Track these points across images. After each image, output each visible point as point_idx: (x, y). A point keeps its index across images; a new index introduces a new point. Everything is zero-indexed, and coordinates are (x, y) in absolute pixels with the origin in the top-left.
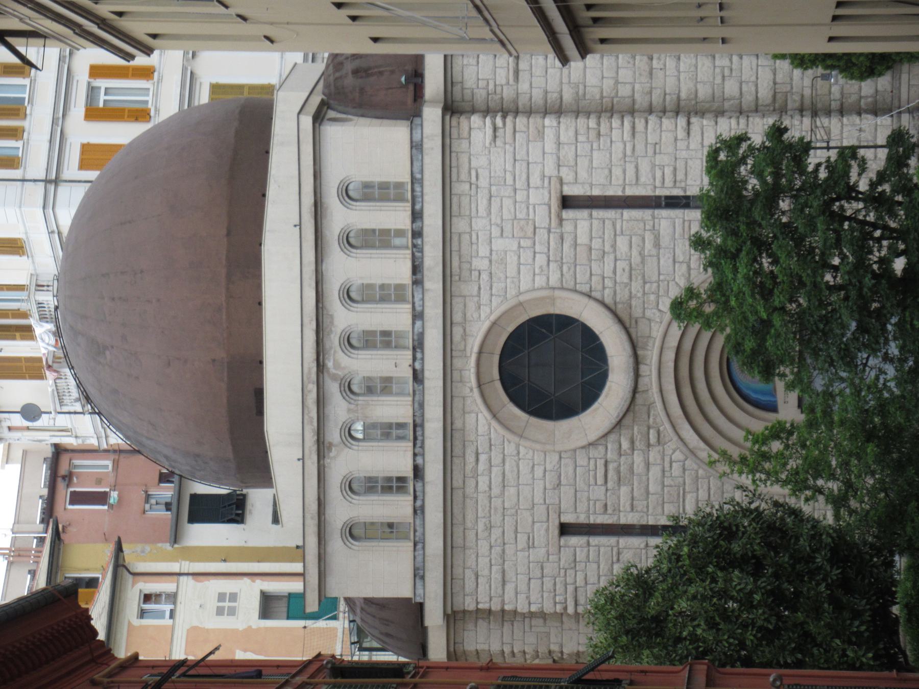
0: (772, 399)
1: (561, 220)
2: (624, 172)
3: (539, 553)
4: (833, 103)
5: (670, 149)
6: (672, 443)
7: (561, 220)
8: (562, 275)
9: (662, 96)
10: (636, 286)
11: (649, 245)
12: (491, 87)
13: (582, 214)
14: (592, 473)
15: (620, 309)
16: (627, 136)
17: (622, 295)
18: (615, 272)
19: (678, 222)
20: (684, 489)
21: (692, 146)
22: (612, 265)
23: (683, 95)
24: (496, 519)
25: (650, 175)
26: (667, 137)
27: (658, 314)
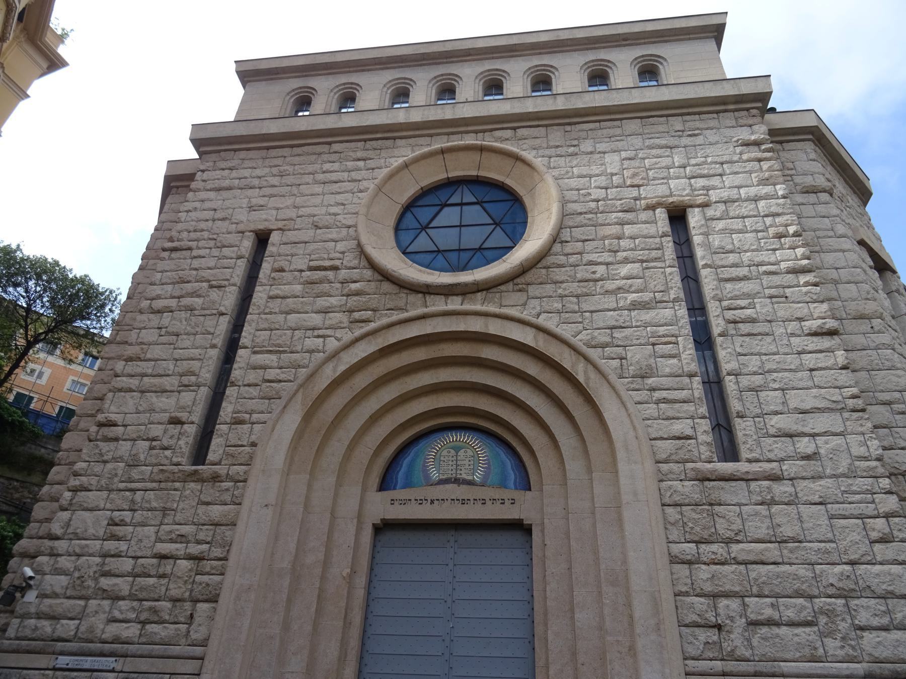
1: (652, 208)
3: (242, 216)
7: (652, 208)
8: (581, 213)
10: (574, 287)
18: (591, 263)
19: (673, 329)
20: (284, 352)
24: (290, 180)
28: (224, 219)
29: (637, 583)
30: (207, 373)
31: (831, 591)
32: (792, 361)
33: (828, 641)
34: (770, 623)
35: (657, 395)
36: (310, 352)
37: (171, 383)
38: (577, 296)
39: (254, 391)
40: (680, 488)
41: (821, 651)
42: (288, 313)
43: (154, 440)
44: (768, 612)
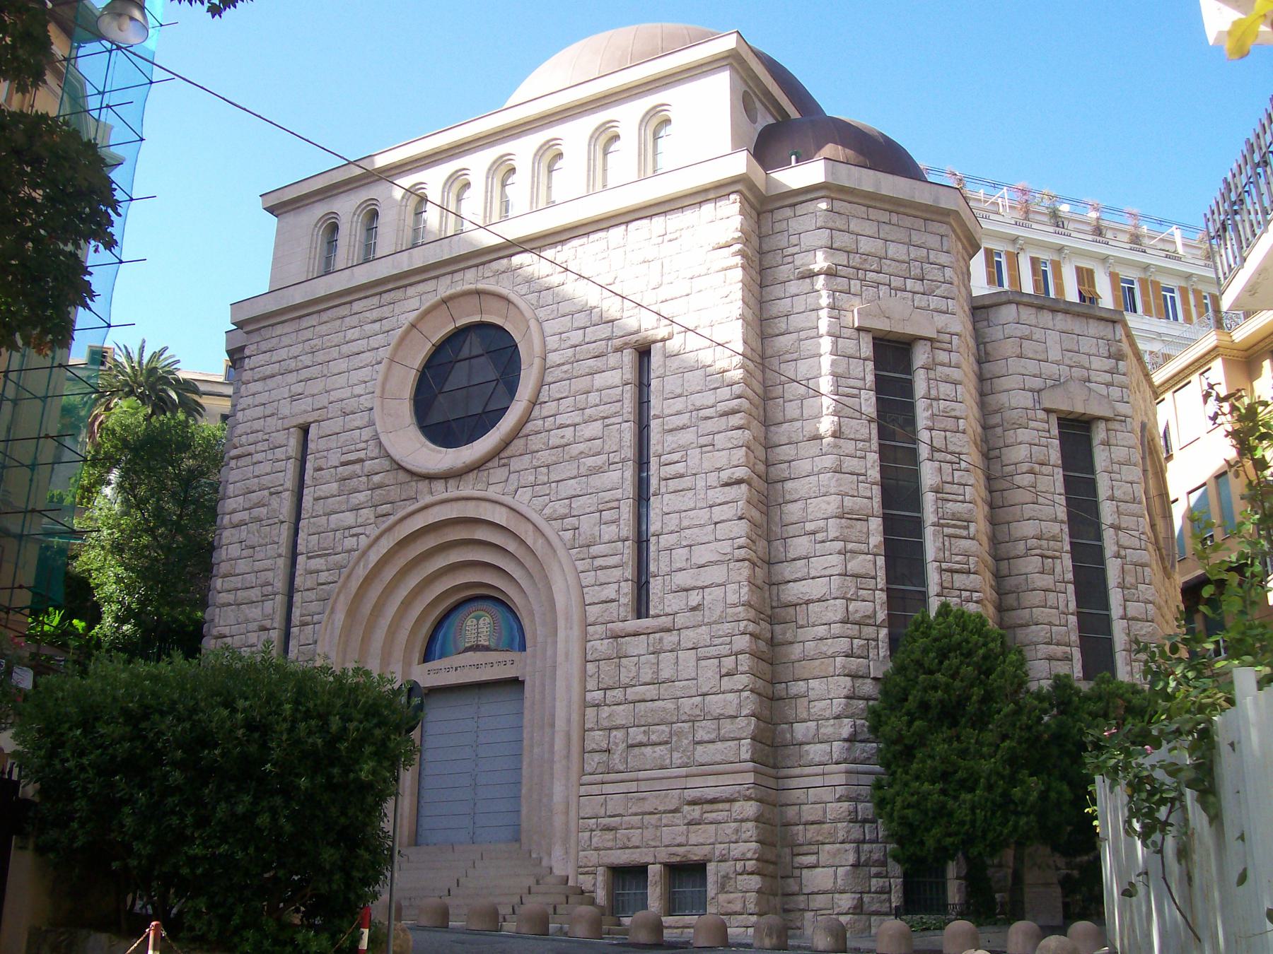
0: (437, 654)
1: (619, 350)
2: (678, 413)
3: (285, 409)
4: (784, 685)
5: (707, 465)
6: (373, 531)
7: (619, 350)
8: (559, 365)
9: (786, 458)
10: (545, 457)
11: (590, 461)
12: (791, 250)
13: (629, 373)
14: (353, 447)
15: (518, 444)
16: (722, 407)
17: (536, 442)
18: (561, 427)
19: (618, 494)
20: (329, 555)
21: (710, 492)
22: (568, 422)
23: (789, 485)
24: (320, 357)
25: (674, 446)
26: (721, 458)
27: (513, 488)
28: (273, 415)
29: (560, 724)
30: (280, 584)
31: (684, 718)
32: (703, 515)
33: (676, 755)
34: (641, 745)
35: (599, 562)
36: (349, 551)
37: (254, 594)
38: (548, 466)
39: (311, 595)
40: (599, 648)
41: (668, 761)
42: (329, 514)
43: (252, 646)
44: (641, 738)
